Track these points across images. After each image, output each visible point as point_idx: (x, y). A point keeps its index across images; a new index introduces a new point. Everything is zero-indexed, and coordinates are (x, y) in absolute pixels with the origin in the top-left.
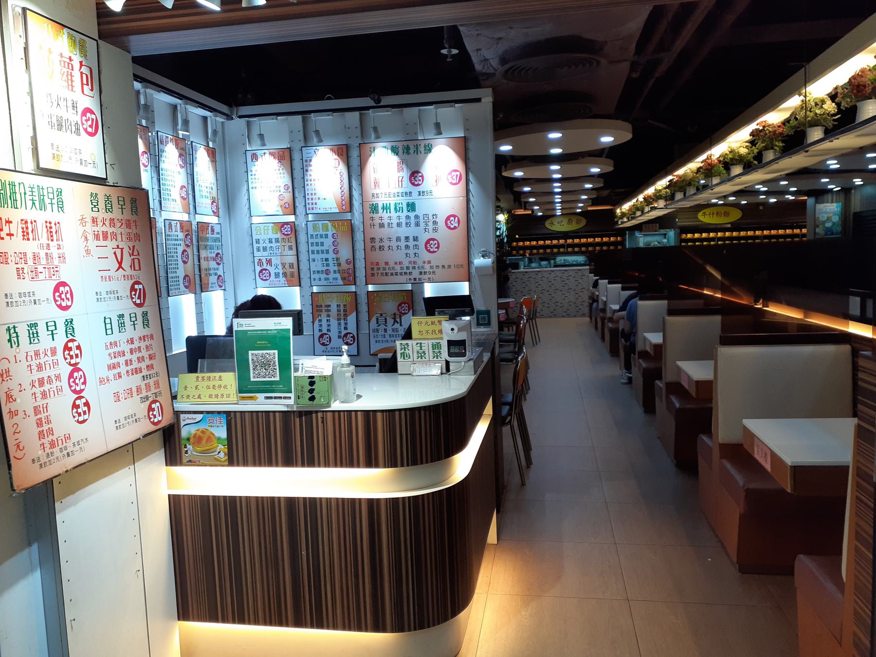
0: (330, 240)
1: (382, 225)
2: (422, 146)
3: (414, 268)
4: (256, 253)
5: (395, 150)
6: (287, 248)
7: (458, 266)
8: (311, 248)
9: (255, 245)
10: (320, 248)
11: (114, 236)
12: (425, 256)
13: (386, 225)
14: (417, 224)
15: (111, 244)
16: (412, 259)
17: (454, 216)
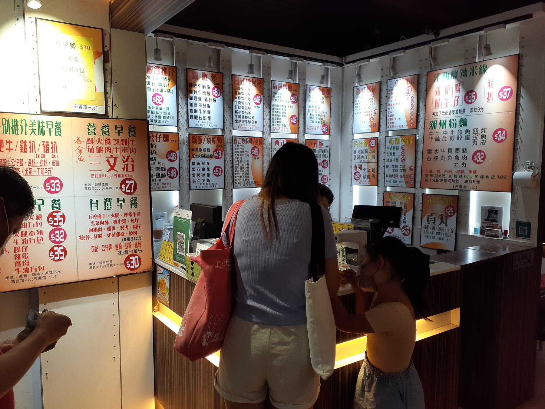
0: (400, 150)
1: (438, 139)
2: (478, 67)
3: (461, 176)
4: (354, 161)
5: (454, 75)
6: (371, 157)
7: (501, 177)
8: (387, 157)
9: (354, 155)
10: (392, 157)
11: (109, 150)
12: (472, 166)
13: (441, 139)
14: (467, 138)
15: (104, 155)
16: (460, 168)
17: (502, 130)
